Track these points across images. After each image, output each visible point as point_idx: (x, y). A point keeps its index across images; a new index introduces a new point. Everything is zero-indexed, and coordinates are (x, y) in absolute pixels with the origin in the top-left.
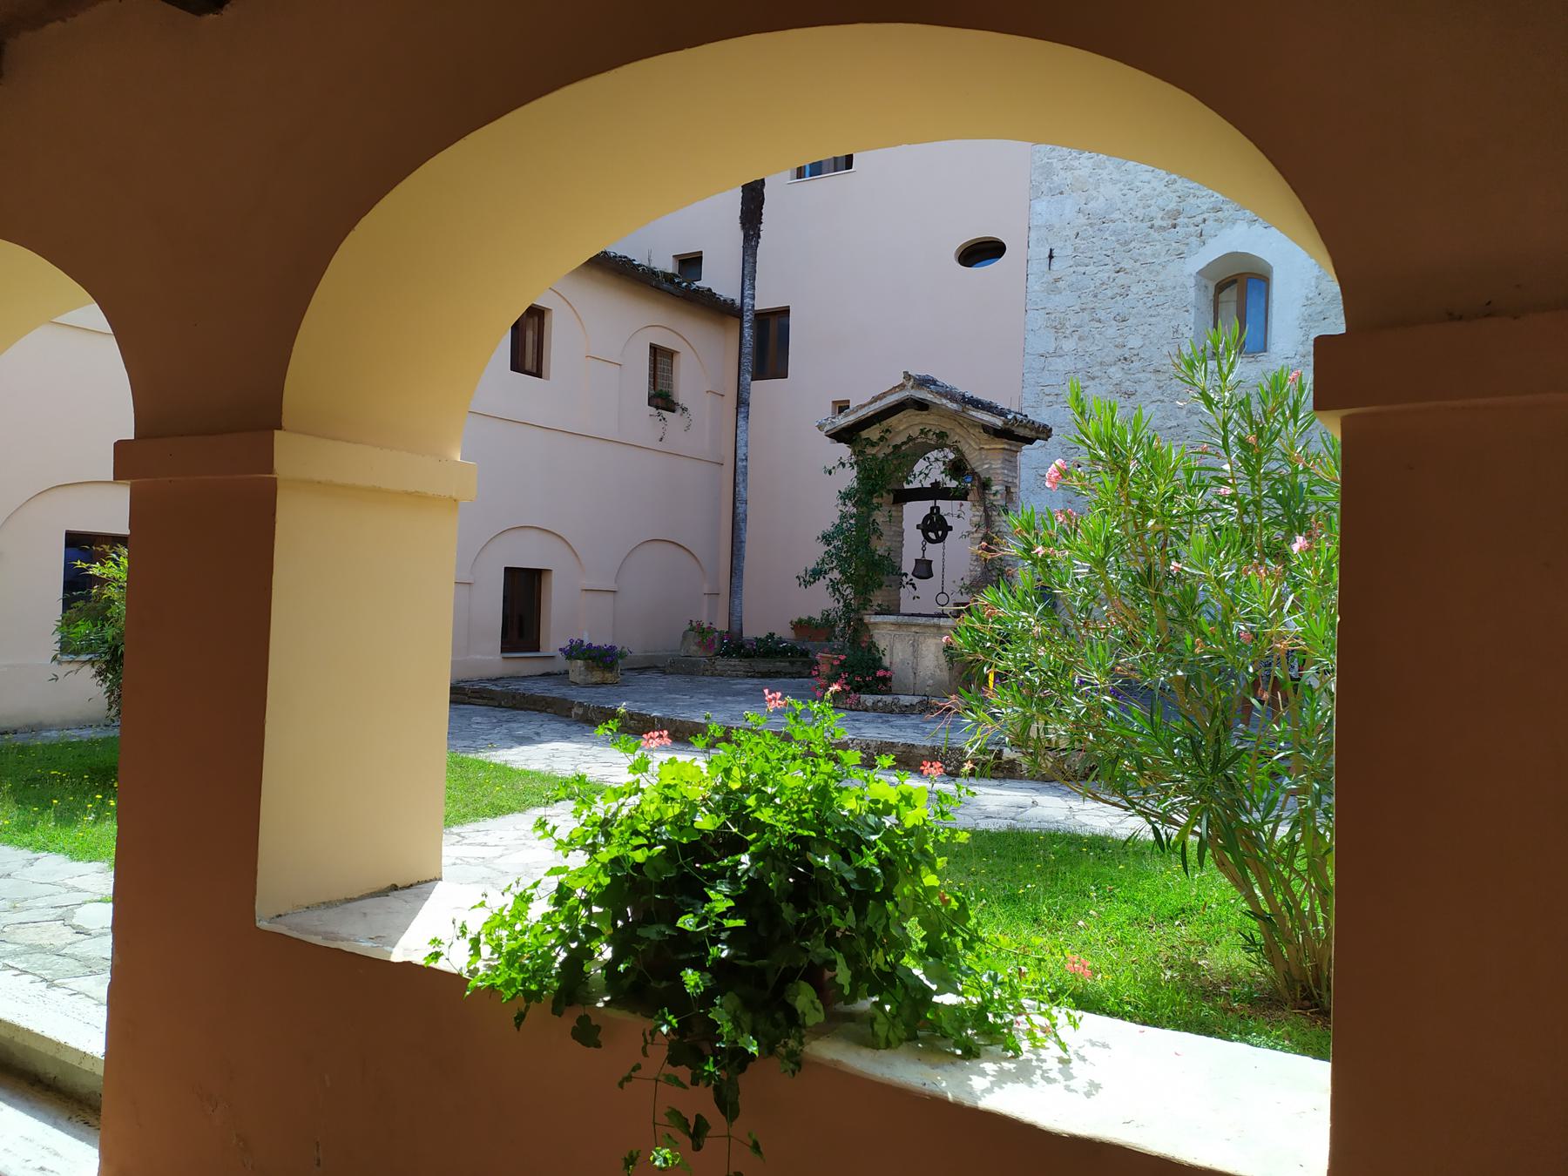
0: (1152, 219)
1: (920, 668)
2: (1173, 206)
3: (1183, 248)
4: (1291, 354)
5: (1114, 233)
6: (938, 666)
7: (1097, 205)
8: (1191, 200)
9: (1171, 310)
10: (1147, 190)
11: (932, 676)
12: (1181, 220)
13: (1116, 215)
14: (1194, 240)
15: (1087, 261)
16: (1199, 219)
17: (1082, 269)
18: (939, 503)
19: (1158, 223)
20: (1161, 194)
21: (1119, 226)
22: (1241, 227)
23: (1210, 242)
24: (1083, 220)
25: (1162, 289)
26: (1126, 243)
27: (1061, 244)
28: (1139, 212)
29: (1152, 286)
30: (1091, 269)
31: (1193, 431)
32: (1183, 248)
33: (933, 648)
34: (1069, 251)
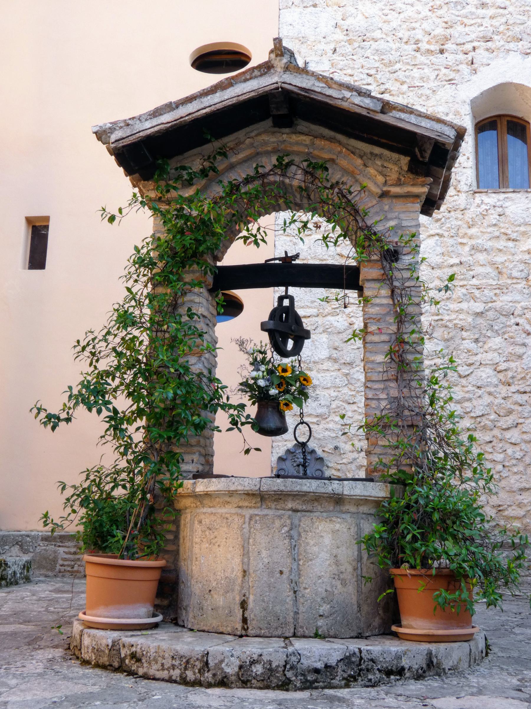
0: (417, 42)
1: (305, 581)
2: (439, 31)
6: (338, 576)
7: (356, 22)
8: (460, 28)
10: (410, 12)
11: (328, 598)
12: (449, 46)
13: (377, 34)
14: (465, 69)
16: (469, 47)
18: (292, 291)
19: (424, 46)
20: (426, 18)
21: (382, 45)
22: (515, 59)
23: (483, 70)
24: (339, 36)
26: (391, 63)
27: (317, 59)
28: (403, 33)
31: (479, 270)
32: (452, 75)
33: (327, 540)
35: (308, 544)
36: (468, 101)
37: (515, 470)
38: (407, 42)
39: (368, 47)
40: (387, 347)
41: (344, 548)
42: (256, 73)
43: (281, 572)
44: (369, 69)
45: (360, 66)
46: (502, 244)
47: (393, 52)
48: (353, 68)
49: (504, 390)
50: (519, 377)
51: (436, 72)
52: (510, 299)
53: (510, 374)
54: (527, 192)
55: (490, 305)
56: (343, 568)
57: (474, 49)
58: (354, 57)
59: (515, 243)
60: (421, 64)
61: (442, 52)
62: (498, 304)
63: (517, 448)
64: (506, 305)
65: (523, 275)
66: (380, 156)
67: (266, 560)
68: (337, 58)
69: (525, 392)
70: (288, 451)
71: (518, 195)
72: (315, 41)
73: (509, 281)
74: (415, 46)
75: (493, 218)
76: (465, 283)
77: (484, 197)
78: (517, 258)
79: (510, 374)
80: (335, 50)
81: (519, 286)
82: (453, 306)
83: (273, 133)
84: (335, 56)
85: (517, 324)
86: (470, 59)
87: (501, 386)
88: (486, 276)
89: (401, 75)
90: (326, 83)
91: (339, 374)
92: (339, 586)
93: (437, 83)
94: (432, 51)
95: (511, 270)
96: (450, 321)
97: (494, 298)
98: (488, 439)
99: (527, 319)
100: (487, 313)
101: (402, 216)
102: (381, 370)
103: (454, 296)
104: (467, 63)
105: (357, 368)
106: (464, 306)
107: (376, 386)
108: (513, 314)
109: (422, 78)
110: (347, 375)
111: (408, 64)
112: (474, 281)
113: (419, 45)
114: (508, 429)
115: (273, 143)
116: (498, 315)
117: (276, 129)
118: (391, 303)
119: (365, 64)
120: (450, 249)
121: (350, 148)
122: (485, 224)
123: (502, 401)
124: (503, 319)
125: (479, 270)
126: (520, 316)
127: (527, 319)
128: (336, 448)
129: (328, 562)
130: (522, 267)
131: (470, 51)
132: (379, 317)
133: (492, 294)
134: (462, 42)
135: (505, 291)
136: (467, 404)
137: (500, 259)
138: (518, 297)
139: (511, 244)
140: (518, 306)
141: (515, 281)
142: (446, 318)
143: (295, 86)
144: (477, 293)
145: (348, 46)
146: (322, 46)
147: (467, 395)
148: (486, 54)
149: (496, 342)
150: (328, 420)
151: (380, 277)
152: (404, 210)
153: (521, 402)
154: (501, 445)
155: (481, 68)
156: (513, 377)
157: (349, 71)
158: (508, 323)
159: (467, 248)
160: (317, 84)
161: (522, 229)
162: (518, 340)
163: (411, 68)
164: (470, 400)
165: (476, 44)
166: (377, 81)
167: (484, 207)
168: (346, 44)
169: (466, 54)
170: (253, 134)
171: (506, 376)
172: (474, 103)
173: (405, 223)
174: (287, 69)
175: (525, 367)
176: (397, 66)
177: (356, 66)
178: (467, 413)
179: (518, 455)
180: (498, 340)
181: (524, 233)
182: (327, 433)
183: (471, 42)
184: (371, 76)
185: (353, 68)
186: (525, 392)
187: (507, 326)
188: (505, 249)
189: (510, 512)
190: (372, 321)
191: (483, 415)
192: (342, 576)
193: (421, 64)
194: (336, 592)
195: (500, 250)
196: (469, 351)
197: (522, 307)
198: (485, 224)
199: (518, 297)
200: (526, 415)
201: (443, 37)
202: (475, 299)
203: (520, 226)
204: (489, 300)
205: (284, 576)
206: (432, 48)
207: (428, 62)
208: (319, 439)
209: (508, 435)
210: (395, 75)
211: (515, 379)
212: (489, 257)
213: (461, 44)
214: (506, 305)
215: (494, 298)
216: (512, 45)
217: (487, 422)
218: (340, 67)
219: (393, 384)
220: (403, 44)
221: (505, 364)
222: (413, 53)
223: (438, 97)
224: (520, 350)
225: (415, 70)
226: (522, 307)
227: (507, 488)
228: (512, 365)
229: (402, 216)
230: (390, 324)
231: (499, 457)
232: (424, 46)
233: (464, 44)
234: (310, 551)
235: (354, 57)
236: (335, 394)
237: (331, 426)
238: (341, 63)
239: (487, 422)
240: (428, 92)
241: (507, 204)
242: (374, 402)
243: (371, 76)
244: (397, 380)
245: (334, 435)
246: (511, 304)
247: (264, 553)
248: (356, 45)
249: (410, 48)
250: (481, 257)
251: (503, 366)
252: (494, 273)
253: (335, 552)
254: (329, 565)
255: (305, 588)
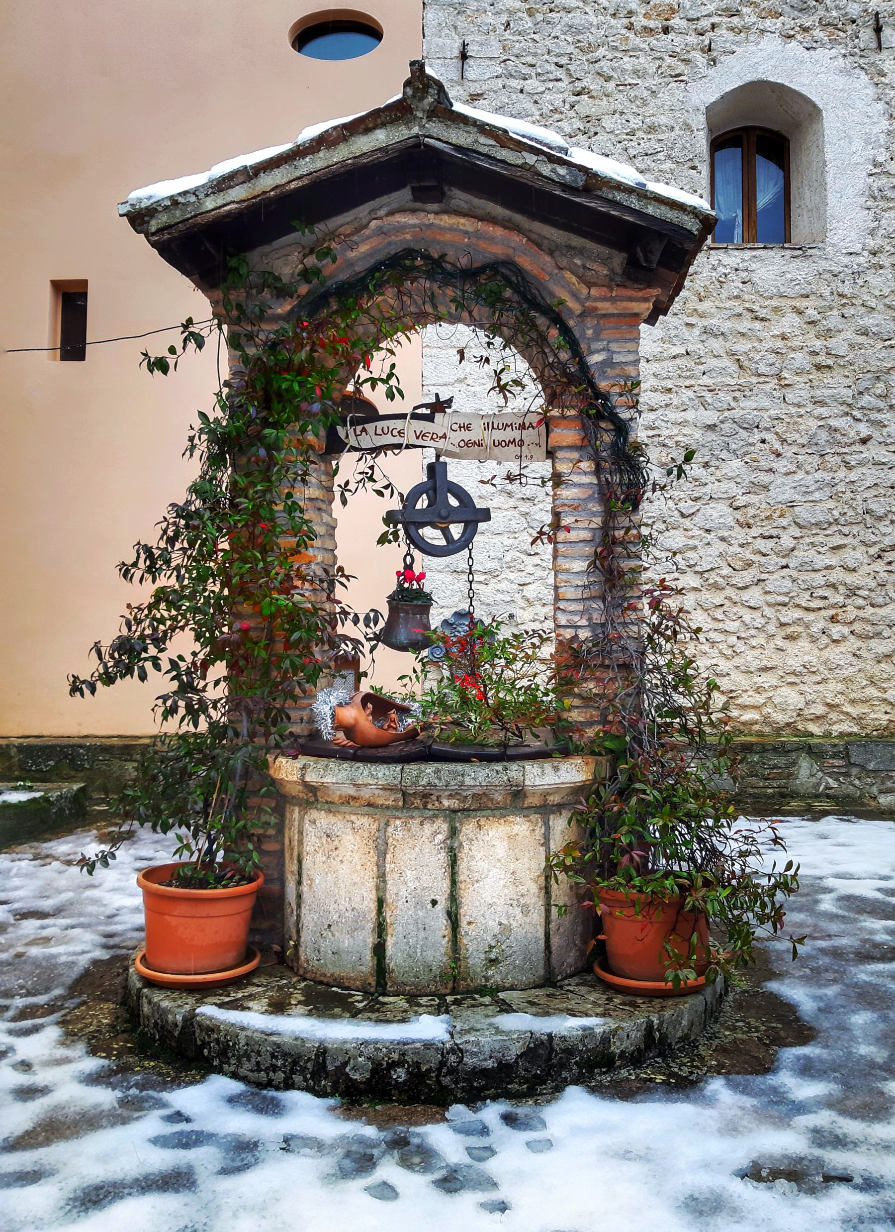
0: (631, 13)
3: (681, 68)
4: (857, 248)
5: (570, 28)
9: (668, 165)
14: (700, 59)
15: (526, 70)
16: (705, 23)
17: (516, 84)
19: (640, 21)
21: (576, 18)
25: (652, 129)
26: (591, 48)
29: (635, 122)
30: (532, 84)
31: (712, 363)
33: (501, 850)
34: (495, 50)
35: (473, 857)
36: (703, 109)
37: (754, 642)
38: (614, 14)
39: (556, 20)
40: (589, 550)
41: (526, 860)
42: (383, 118)
43: (434, 903)
44: (557, 55)
45: (545, 51)
46: (745, 325)
47: (593, 30)
48: (535, 54)
49: (740, 535)
50: (763, 516)
51: (658, 63)
52: (754, 405)
53: (751, 511)
54: (783, 248)
55: (726, 414)
56: (523, 889)
57: (713, 26)
58: (536, 37)
59: (763, 324)
60: (633, 50)
61: (666, 30)
62: (737, 414)
63: (757, 614)
64: (749, 414)
65: (774, 370)
66: (581, 252)
67: (412, 886)
68: (510, 37)
69: (771, 537)
70: (445, 622)
71: (771, 253)
72: (478, 10)
73: (754, 380)
74: (626, 21)
75: (734, 286)
76: (692, 382)
77: (721, 255)
78: (766, 345)
79: (751, 511)
80: (508, 24)
81: (767, 387)
82: (673, 415)
83: (414, 211)
84: (507, 35)
85: (763, 441)
86: (707, 42)
87: (738, 528)
88: (722, 371)
89: (605, 66)
90: (496, 138)
91: (515, 513)
92: (519, 916)
93: (658, 80)
94: (651, 30)
95: (756, 363)
96: (670, 437)
97: (733, 404)
98: (718, 601)
99: (777, 434)
100: (722, 426)
101: (614, 347)
102: (580, 583)
103: (675, 402)
104: (702, 50)
105: (541, 506)
106: (690, 415)
107: (573, 607)
108: (757, 427)
109: (636, 72)
110: (525, 515)
111: (616, 48)
112: (705, 380)
113: (632, 19)
114: (746, 588)
115: (414, 226)
116: (737, 429)
117: (418, 205)
118: (596, 482)
119: (552, 47)
120: (673, 333)
121: (534, 237)
122: (723, 296)
123: (740, 549)
124: (743, 434)
125: (712, 363)
126: (766, 429)
127: (777, 434)
128: (511, 616)
129: (502, 883)
130: (772, 358)
131: (706, 31)
132: (576, 503)
133: (729, 398)
134: (695, 17)
135: (748, 393)
136: (690, 554)
137: (742, 346)
138: (766, 403)
139: (757, 325)
140: (766, 415)
141: (761, 380)
142: (666, 433)
143: (447, 143)
144: (708, 396)
145: (528, 18)
146: (489, 18)
147: (691, 542)
148: (730, 36)
149: (735, 466)
150: (500, 578)
151: (579, 443)
152: (618, 336)
153: (764, 550)
154: (735, 610)
155: (722, 58)
156: (754, 517)
157: (530, 59)
158: (751, 440)
159: (696, 332)
160: (482, 140)
161: (774, 303)
162: (765, 464)
163: (619, 55)
164: (695, 548)
165: (715, 19)
166: (571, 75)
167: (721, 270)
168: (525, 15)
169: (702, 35)
170: (382, 213)
171: (746, 514)
172: (710, 110)
173: (617, 358)
174: (432, 114)
175: (772, 502)
176: (601, 52)
177: (539, 52)
178: (690, 567)
179: (759, 622)
180: (737, 463)
181: (776, 309)
182: (500, 596)
183: (709, 16)
184: (561, 66)
185: (535, 54)
186: (771, 537)
187: (750, 444)
188: (749, 333)
189: (744, 700)
190: (567, 509)
191: (712, 569)
192: (522, 901)
193: (633, 50)
194: (514, 924)
195: (743, 335)
196: (696, 480)
197: (770, 417)
198: (723, 296)
199: (766, 403)
200: (771, 568)
201: (667, 8)
202: (705, 405)
203: (771, 298)
204: (725, 406)
205: (439, 907)
206: (652, 24)
207: (642, 46)
208: (488, 605)
209: (745, 596)
210: (597, 65)
211: (757, 519)
212: (727, 345)
213: (693, 20)
214: (749, 414)
215: (733, 404)
216: (768, 23)
217: (718, 579)
218: (516, 51)
219: (597, 605)
220: (608, 17)
221: (744, 498)
222: (624, 31)
223: (659, 102)
224: (765, 478)
225: (626, 59)
226: (770, 417)
227: (743, 668)
228: (753, 499)
229: (614, 347)
230: (594, 514)
231: (732, 626)
232: (640, 21)
233: (698, 19)
234: (475, 868)
235: (536, 37)
236: (511, 541)
237: (504, 586)
238: (517, 45)
239: (718, 579)
240: (646, 93)
241: (754, 266)
242: (569, 630)
243: (561, 66)
244: (604, 599)
245: (508, 599)
246: (755, 413)
247: (409, 875)
248: (539, 17)
249: (619, 24)
250: (716, 344)
251: (741, 501)
252: (735, 367)
253: (512, 867)
254: (504, 886)
255: (469, 923)
